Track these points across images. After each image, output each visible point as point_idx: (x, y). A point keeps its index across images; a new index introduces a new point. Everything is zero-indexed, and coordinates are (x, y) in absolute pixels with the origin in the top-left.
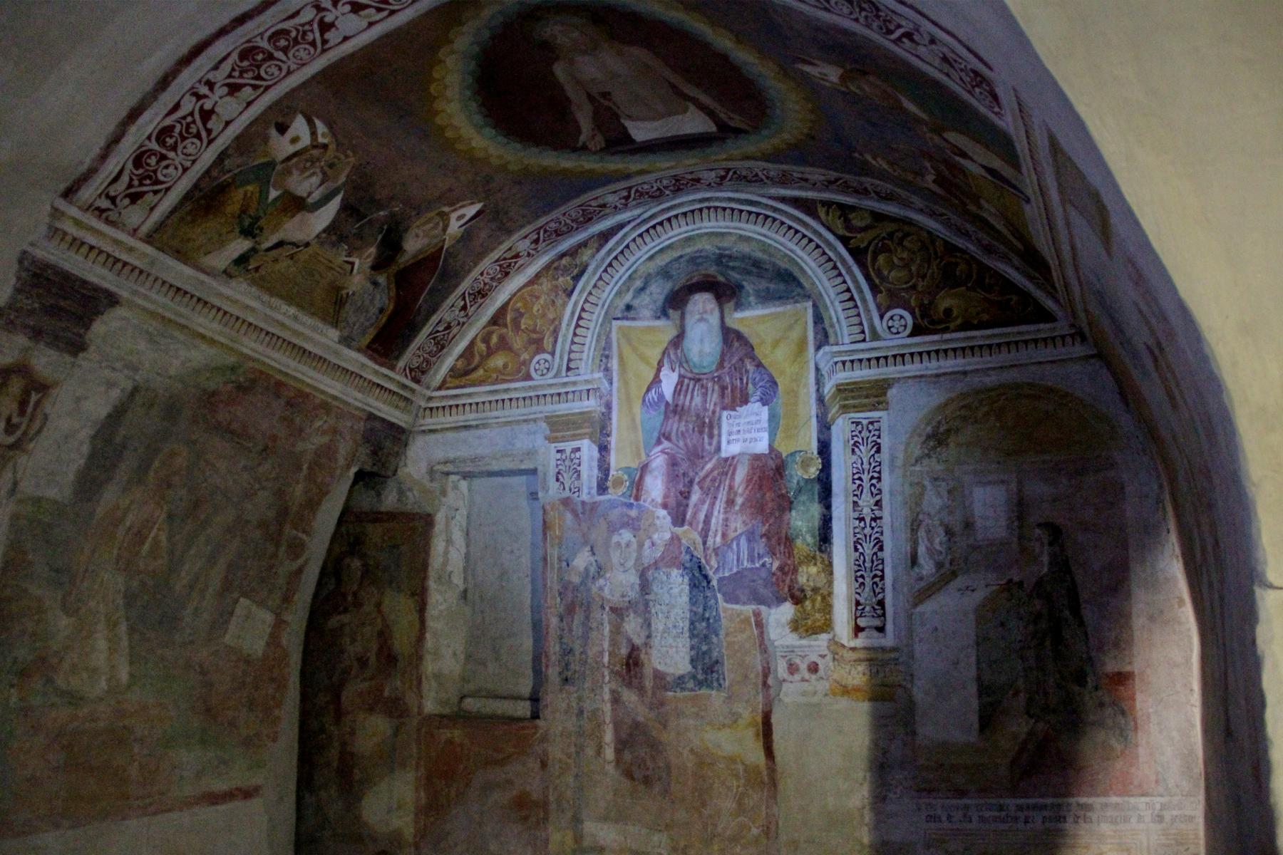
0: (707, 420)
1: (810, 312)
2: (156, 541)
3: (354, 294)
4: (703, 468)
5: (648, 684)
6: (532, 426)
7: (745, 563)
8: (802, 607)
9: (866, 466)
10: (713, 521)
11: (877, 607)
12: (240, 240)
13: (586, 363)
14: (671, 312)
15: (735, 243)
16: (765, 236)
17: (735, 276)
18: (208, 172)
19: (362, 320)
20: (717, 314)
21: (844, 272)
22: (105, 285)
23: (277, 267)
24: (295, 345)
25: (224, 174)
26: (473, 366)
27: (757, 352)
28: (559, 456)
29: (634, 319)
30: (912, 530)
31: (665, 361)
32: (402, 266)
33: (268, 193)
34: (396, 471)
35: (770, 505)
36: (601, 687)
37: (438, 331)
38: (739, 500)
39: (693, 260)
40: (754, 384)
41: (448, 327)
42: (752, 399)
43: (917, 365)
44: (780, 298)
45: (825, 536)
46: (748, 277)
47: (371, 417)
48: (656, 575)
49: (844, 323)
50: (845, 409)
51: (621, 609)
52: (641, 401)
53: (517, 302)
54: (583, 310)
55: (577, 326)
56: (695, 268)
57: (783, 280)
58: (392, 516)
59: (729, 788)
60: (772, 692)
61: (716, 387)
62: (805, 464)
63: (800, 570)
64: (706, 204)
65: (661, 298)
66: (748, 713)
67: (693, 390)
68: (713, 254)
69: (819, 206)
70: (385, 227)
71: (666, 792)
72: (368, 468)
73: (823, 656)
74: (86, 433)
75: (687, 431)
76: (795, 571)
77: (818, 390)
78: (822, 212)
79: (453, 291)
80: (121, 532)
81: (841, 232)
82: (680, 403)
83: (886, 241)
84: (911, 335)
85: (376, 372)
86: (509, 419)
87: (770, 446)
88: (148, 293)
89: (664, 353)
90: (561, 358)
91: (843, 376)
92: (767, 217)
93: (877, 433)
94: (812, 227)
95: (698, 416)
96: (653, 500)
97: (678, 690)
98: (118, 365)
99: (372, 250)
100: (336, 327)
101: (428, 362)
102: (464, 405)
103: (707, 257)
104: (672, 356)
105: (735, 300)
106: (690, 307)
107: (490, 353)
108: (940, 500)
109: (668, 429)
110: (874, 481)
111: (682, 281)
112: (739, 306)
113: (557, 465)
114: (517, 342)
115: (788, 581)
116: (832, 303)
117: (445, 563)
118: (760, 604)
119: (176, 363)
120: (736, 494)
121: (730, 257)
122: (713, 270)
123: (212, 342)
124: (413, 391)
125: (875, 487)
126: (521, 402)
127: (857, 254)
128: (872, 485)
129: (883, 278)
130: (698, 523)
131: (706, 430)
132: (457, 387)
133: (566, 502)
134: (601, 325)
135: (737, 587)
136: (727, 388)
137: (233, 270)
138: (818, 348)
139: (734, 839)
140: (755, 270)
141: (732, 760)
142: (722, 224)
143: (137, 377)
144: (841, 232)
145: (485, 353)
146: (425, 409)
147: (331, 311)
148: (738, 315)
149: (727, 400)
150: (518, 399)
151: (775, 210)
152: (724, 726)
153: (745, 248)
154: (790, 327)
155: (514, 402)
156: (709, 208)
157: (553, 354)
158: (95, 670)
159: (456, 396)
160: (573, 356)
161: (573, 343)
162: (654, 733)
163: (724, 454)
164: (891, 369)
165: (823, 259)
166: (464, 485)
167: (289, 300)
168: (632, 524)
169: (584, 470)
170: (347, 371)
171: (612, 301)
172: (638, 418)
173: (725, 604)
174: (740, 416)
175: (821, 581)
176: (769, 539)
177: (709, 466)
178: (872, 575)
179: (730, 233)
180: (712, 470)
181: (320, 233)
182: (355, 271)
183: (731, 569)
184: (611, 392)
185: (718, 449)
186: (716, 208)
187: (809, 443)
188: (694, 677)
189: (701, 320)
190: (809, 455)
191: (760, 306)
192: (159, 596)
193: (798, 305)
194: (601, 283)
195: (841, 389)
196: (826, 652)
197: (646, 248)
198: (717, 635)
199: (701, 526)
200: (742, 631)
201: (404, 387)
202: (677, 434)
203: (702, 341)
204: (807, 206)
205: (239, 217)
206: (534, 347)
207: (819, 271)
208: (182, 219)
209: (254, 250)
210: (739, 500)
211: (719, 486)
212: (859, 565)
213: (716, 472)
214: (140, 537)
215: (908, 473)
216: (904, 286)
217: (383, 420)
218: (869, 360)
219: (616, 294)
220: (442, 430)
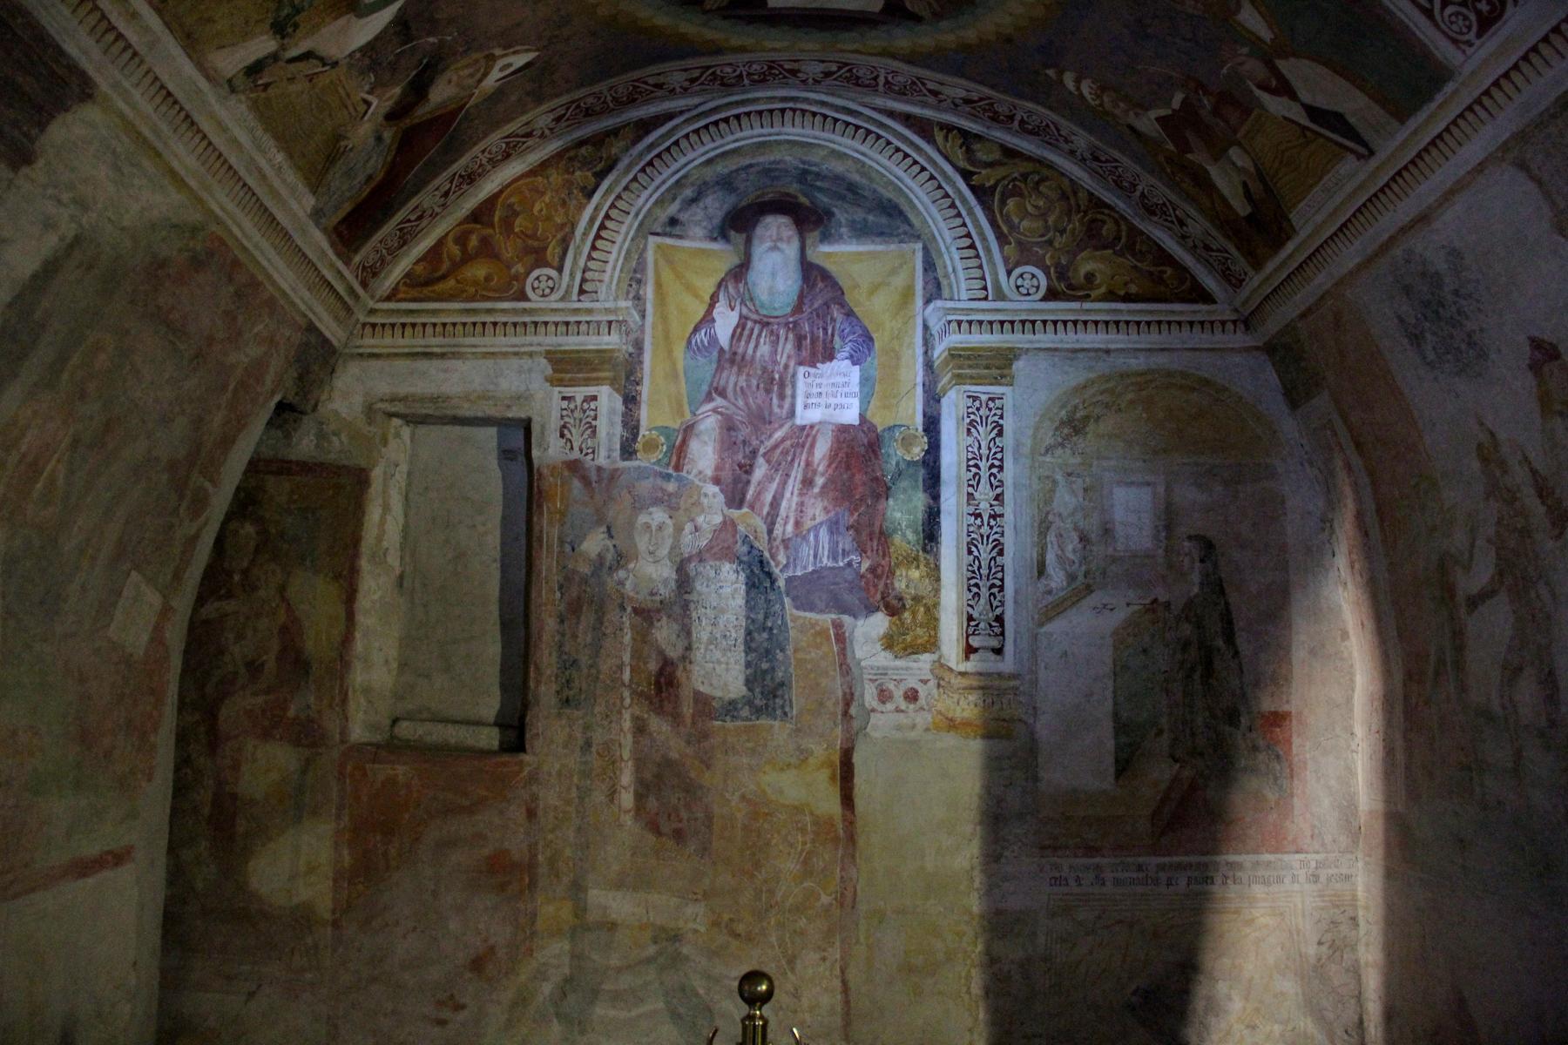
0: (777, 376)
1: (919, 256)
2: (52, 481)
4: (770, 436)
5: (687, 710)
6: (526, 363)
7: (825, 560)
8: (900, 620)
9: (984, 451)
10: (784, 504)
11: (994, 624)
13: (609, 287)
14: (733, 233)
16: (863, 154)
17: (823, 199)
20: (796, 244)
21: (964, 213)
26: (440, 273)
27: (847, 298)
28: (565, 404)
29: (680, 237)
30: (1040, 533)
31: (721, 296)
34: (316, 405)
35: (860, 489)
36: (620, 712)
37: (409, 221)
38: (820, 481)
39: (768, 172)
40: (843, 338)
41: (420, 218)
42: (839, 356)
43: (1050, 335)
44: (881, 234)
45: (930, 532)
46: (840, 202)
48: (701, 569)
49: (961, 275)
50: (959, 379)
51: (649, 611)
52: (684, 343)
53: (510, 196)
54: (607, 217)
55: (598, 237)
56: (769, 183)
57: (890, 215)
58: (306, 467)
59: (791, 845)
60: (856, 724)
61: (791, 336)
62: (907, 442)
63: (898, 573)
64: (791, 105)
65: (720, 214)
66: (822, 750)
67: (759, 335)
69: (936, 129)
71: (704, 850)
72: (291, 398)
73: (925, 682)
75: (749, 386)
76: (892, 573)
77: (926, 353)
78: (939, 137)
79: (446, 169)
81: (963, 164)
82: (740, 351)
83: (1017, 183)
84: (1044, 299)
86: (492, 350)
87: (862, 417)
89: (719, 286)
90: (572, 275)
91: (956, 339)
92: (869, 132)
93: (999, 412)
94: (926, 153)
95: (764, 370)
96: (700, 473)
97: (728, 718)
101: (382, 260)
102: (424, 325)
103: (787, 171)
104: (731, 290)
105: (821, 229)
106: (759, 231)
107: (467, 258)
108: (1074, 500)
109: (722, 383)
110: (994, 470)
111: (751, 198)
112: (826, 237)
113: (562, 417)
114: (508, 249)
115: (881, 586)
116: (947, 248)
117: (379, 539)
118: (843, 613)
120: (815, 472)
121: (818, 175)
122: (794, 188)
124: (357, 297)
125: (995, 478)
126: (510, 329)
127: (980, 192)
128: (991, 474)
129: (1012, 227)
130: (763, 505)
131: (776, 388)
132: (414, 300)
133: (574, 467)
134: (632, 240)
135: (809, 590)
136: (805, 338)
138: (927, 302)
139: (798, 909)
140: (850, 196)
141: (797, 810)
142: (808, 131)
144: (963, 164)
145: (458, 259)
146: (364, 325)
148: (825, 248)
149: (805, 353)
150: (505, 324)
151: (882, 125)
152: (789, 765)
153: (838, 167)
154: (894, 272)
155: (499, 329)
156: (794, 110)
157: (560, 269)
159: (411, 312)
160: (589, 275)
161: (590, 258)
162: (693, 775)
163: (799, 422)
164: (1018, 336)
165: (940, 193)
166: (406, 432)
168: (668, 502)
169: (602, 425)
171: (650, 210)
172: (680, 366)
173: (794, 611)
174: (822, 376)
175: (925, 587)
176: (857, 531)
177: (778, 435)
178: (989, 584)
179: (819, 145)
180: (783, 440)
183: (805, 568)
184: (642, 328)
185: (792, 413)
186: (804, 111)
187: (912, 417)
188: (750, 703)
189: (775, 248)
190: (912, 431)
193: (904, 245)
194: (635, 185)
195: (954, 355)
196: (930, 677)
197: (702, 150)
198: (782, 650)
199: (766, 510)
200: (818, 647)
201: (352, 291)
202: (735, 390)
203: (774, 275)
204: (923, 128)
206: (530, 259)
207: (934, 210)
210: (820, 481)
211: (793, 460)
212: (973, 572)
213: (788, 443)
214: (35, 469)
215: (1037, 464)
216: (1040, 239)
217: (321, 334)
218: (991, 323)
219: (656, 203)
220: (389, 356)
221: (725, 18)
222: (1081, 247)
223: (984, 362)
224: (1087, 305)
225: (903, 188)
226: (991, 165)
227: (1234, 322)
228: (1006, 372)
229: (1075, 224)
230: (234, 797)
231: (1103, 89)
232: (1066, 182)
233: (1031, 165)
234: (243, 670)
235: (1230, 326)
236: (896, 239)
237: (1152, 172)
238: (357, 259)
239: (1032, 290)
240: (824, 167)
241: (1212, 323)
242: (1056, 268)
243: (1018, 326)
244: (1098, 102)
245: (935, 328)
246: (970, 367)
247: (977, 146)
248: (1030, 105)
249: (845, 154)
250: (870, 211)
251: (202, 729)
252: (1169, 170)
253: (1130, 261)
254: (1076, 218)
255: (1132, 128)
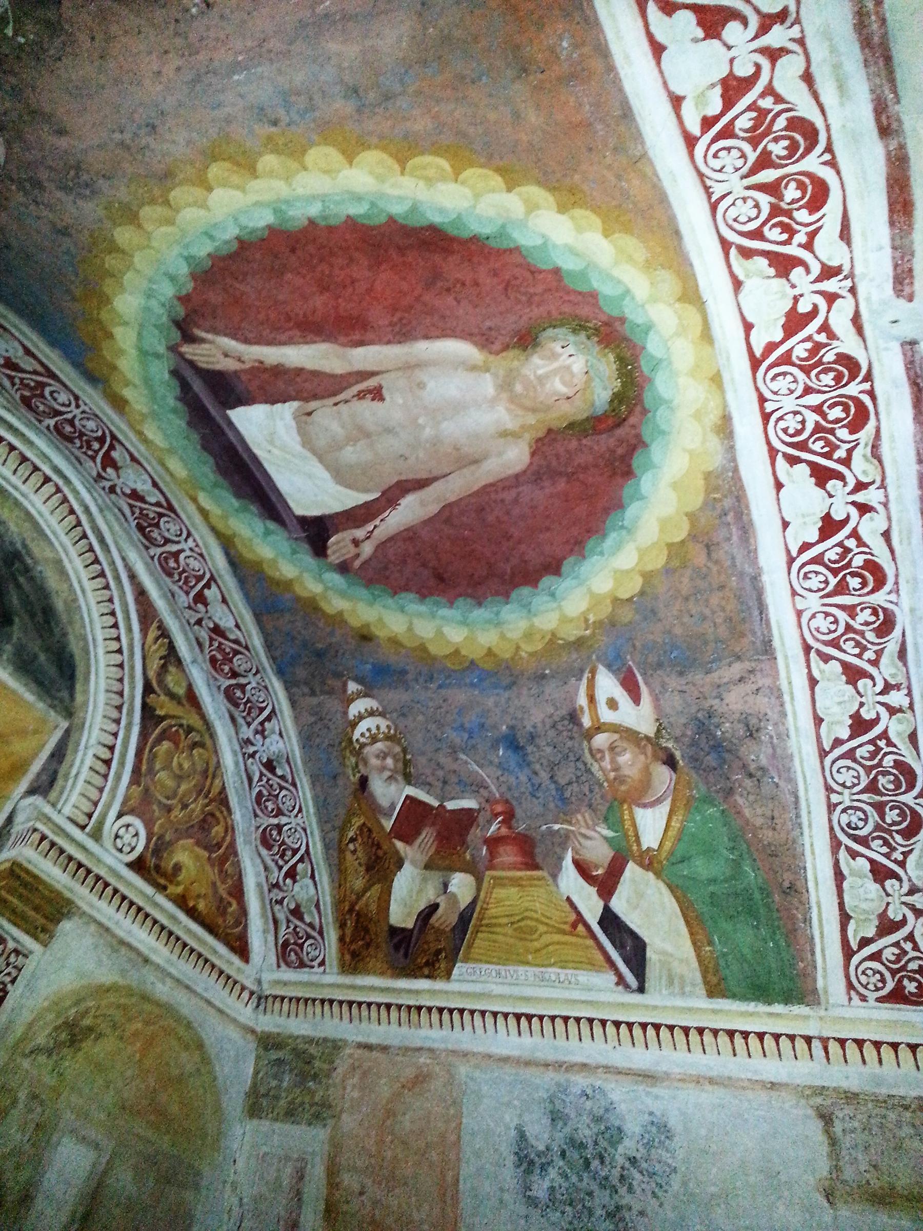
1: (58, 735)
15: (47, 560)
16: (83, 591)
17: (15, 600)
21: (123, 723)
46: (26, 618)
57: (60, 668)
68: (11, 543)
69: (155, 625)
78: (153, 633)
81: (151, 674)
84: (130, 865)
92: (102, 574)
121: (27, 570)
129: (151, 771)
138: (31, 792)
140: (40, 618)
142: (53, 521)
144: (151, 674)
151: (117, 578)
153: (53, 582)
165: (116, 686)
179: (51, 543)
186: (65, 500)
191: (10, 668)
193: (52, 713)
204: (147, 613)
207: (102, 697)
221: (175, 373)
222: (187, 833)
223: (37, 901)
224: (160, 899)
225: (92, 654)
226: (172, 696)
227: (252, 993)
228: (50, 926)
229: (197, 807)
231: (388, 738)
232: (215, 759)
233: (201, 723)
235: (246, 995)
236: (49, 701)
237: (323, 821)
239: (127, 849)
240: (39, 568)
241: (235, 982)
242: (158, 839)
243: (90, 880)
244: (362, 740)
245: (19, 826)
246: (20, 897)
247: (172, 669)
248: (277, 686)
249: (68, 575)
250: (47, 650)
252: (351, 834)
253: (212, 874)
254: (202, 801)
255: (364, 782)
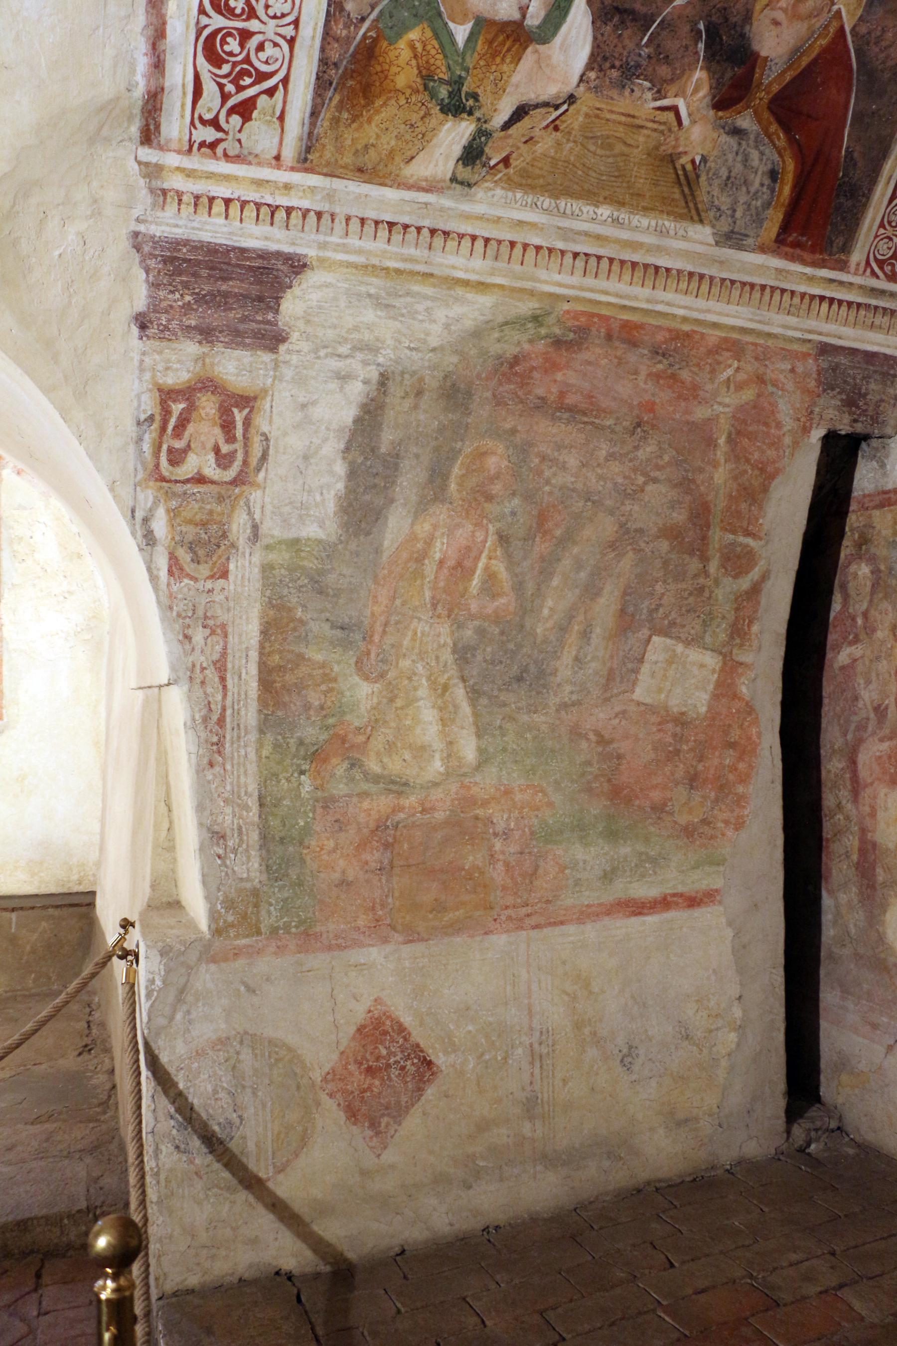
3: (704, 159)
12: (449, 125)
18: (327, 33)
19: (743, 198)
22: (273, 247)
23: (540, 148)
24: (634, 265)
25: (357, 27)
32: (776, 88)
33: (451, 35)
47: (825, 349)
70: (701, 26)
74: (332, 447)
80: (430, 568)
85: (811, 279)
88: (345, 241)
98: (344, 350)
99: (699, 75)
100: (701, 221)
119: (436, 329)
123: (482, 287)
137: (464, 173)
143: (381, 360)
147: (677, 195)
158: (423, 748)
167: (590, 195)
170: (752, 286)
181: (582, 76)
182: (686, 121)
192: (511, 646)
205: (426, 87)
208: (336, 121)
209: (482, 134)
217: (853, 351)
230: (874, 845)
234: (872, 715)
238: (857, 257)
251: (848, 776)
